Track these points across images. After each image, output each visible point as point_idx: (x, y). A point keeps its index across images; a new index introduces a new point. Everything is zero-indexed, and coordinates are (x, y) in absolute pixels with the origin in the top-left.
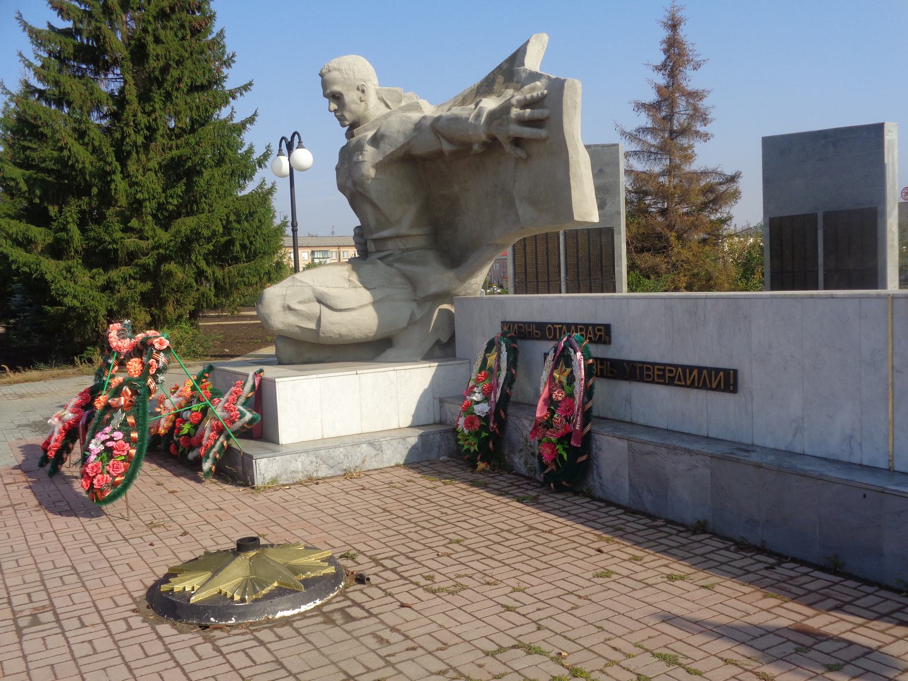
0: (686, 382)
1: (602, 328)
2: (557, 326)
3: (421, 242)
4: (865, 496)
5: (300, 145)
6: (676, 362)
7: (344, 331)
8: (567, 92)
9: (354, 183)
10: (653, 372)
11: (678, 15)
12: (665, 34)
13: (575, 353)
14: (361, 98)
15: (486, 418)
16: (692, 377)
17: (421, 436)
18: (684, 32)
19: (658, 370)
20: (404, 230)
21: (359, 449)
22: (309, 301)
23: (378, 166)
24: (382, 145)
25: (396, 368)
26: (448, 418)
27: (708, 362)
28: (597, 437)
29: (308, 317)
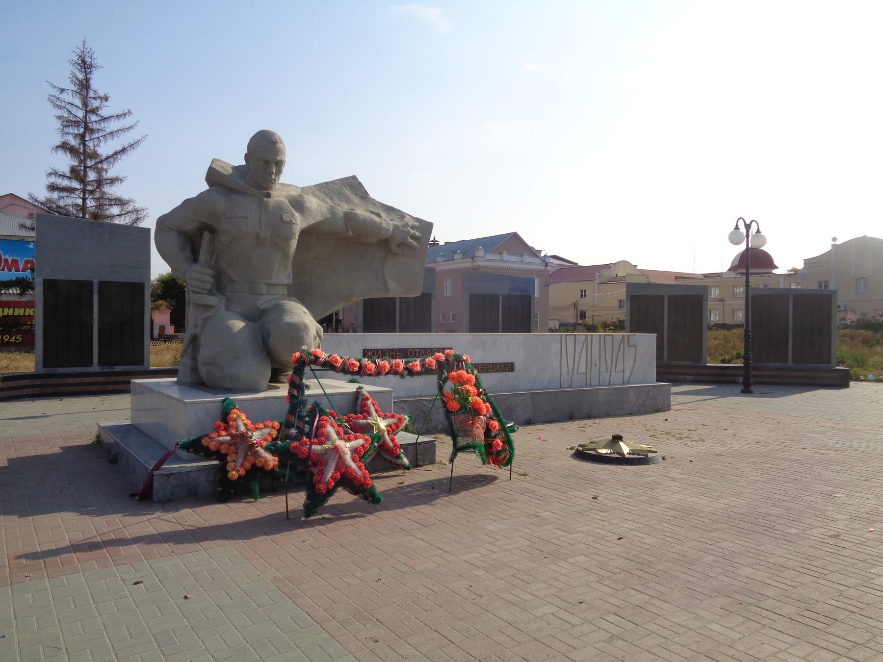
2: (417, 350)
19: (481, 366)
27: (501, 361)
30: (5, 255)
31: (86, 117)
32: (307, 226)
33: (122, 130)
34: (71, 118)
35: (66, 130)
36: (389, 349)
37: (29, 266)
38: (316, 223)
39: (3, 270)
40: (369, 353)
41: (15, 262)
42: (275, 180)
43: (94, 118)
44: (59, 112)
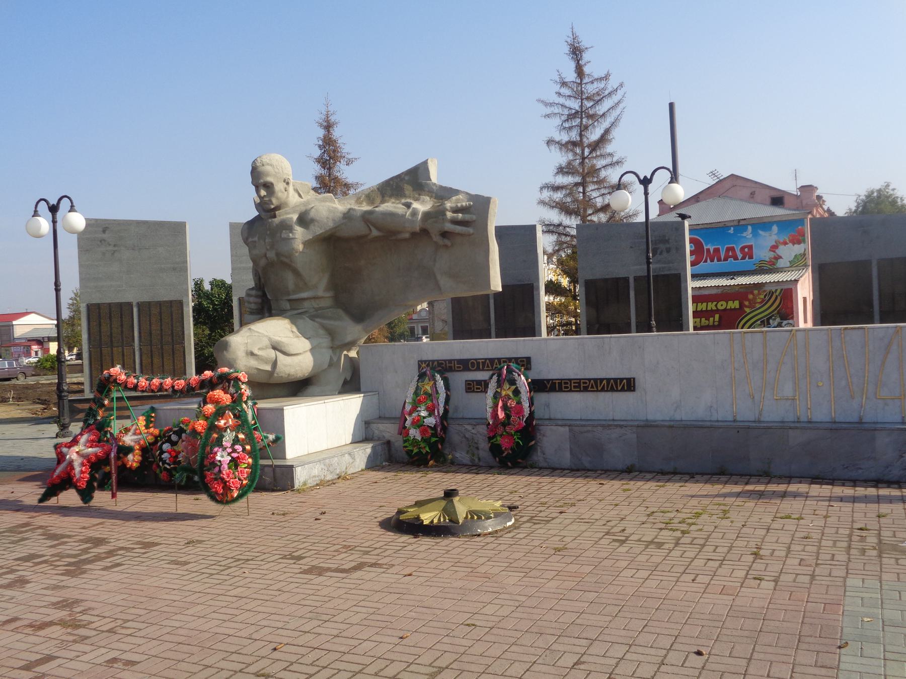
0: (597, 387)
1: (525, 359)
2: (480, 361)
3: (327, 303)
4: (738, 432)
5: (72, 209)
6: (587, 377)
7: (292, 371)
8: (492, 206)
9: (278, 255)
10: (571, 385)
11: (332, 119)
12: (321, 133)
13: (519, 375)
14: (286, 188)
15: (434, 428)
16: (602, 385)
17: (372, 447)
18: (336, 133)
19: (574, 383)
20: (320, 293)
21: (344, 458)
22: (267, 348)
23: (306, 244)
24: (312, 227)
25: (344, 398)
26: (375, 435)
28: (541, 428)
29: (265, 361)
30: (707, 245)
31: (581, 106)
32: (313, 238)
33: (612, 108)
34: (566, 112)
35: (567, 125)
36: (447, 360)
37: (730, 254)
38: (327, 231)
39: (706, 261)
40: (424, 365)
41: (717, 251)
42: (270, 201)
43: (588, 104)
44: (549, 110)
